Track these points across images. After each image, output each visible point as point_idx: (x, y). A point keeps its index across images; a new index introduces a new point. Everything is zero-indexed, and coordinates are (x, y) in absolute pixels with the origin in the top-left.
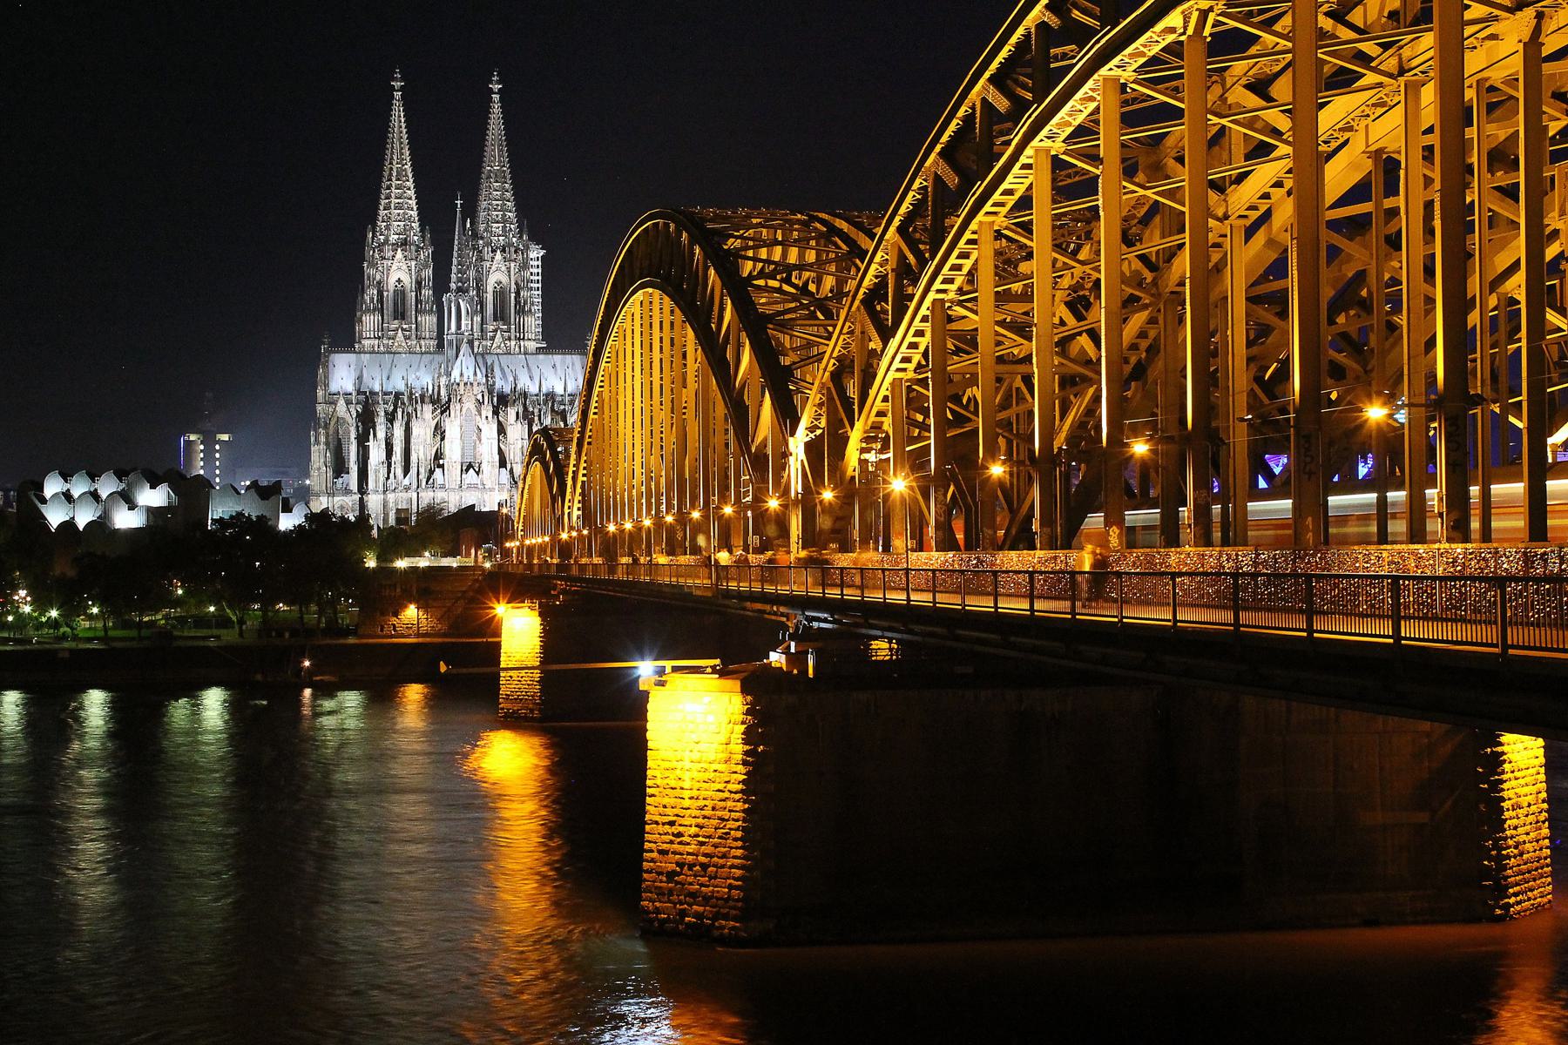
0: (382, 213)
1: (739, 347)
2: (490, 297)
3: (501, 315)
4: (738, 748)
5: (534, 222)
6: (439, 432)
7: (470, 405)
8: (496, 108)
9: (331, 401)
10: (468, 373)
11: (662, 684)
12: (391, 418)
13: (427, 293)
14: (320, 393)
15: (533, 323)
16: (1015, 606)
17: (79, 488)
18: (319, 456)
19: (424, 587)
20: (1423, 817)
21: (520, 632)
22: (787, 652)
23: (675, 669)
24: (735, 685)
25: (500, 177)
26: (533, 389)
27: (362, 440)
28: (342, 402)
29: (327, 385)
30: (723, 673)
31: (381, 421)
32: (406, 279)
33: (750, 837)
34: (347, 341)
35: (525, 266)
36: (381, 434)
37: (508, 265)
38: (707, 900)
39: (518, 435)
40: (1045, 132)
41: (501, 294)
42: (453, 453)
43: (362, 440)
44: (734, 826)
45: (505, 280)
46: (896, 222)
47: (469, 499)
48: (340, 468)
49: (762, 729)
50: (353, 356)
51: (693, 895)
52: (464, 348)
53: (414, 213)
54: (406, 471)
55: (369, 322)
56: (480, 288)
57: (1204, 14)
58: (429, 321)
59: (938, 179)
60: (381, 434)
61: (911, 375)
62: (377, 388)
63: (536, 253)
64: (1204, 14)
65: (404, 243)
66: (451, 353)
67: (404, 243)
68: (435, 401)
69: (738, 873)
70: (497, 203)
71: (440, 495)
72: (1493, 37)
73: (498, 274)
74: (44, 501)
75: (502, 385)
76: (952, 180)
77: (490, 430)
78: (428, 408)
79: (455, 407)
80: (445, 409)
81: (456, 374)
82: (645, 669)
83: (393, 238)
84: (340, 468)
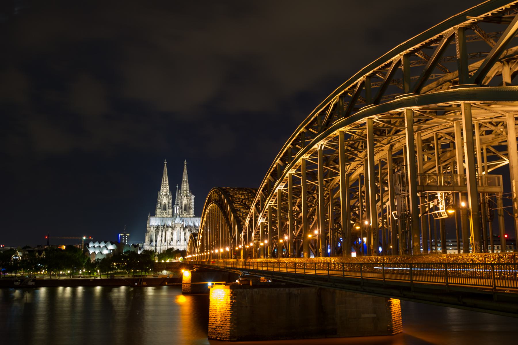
0: (162, 189)
1: (231, 215)
2: (183, 206)
3: (185, 210)
4: (229, 301)
5: (193, 190)
6: (172, 234)
7: (179, 228)
8: (185, 168)
11: (212, 287)
13: (170, 205)
14: (148, 225)
15: (192, 211)
16: (284, 270)
17: (96, 245)
18: (147, 239)
19: (168, 267)
20: (375, 315)
21: (186, 275)
22: (240, 280)
23: (216, 284)
24: (229, 287)
25: (186, 181)
26: (192, 225)
27: (156, 236)
28: (152, 228)
30: (226, 285)
31: (160, 231)
33: (231, 321)
34: (154, 214)
35: (191, 199)
36: (160, 234)
37: (187, 198)
38: (222, 334)
39: (188, 234)
40: (291, 170)
41: (186, 206)
42: (175, 238)
43: (156, 236)
44: (228, 318)
45: (186, 202)
46: (262, 189)
47: (178, 247)
48: (151, 241)
49: (234, 296)
50: (154, 218)
51: (219, 333)
52: (178, 216)
53: (168, 189)
54: (165, 242)
55: (158, 211)
56: (181, 204)
57: (322, 145)
58: (171, 211)
59: (269, 180)
60: (160, 234)
61: (264, 221)
64: (322, 145)
65: (166, 195)
66: (175, 217)
67: (166, 195)
68: (171, 227)
69: (229, 328)
70: (185, 187)
71: (172, 247)
72: (383, 150)
73: (185, 201)
74: (89, 248)
75: (185, 224)
76: (272, 180)
77: (183, 233)
78: (170, 229)
79: (175, 229)
81: (176, 222)
82: (210, 284)
83: (164, 194)
84: (151, 241)
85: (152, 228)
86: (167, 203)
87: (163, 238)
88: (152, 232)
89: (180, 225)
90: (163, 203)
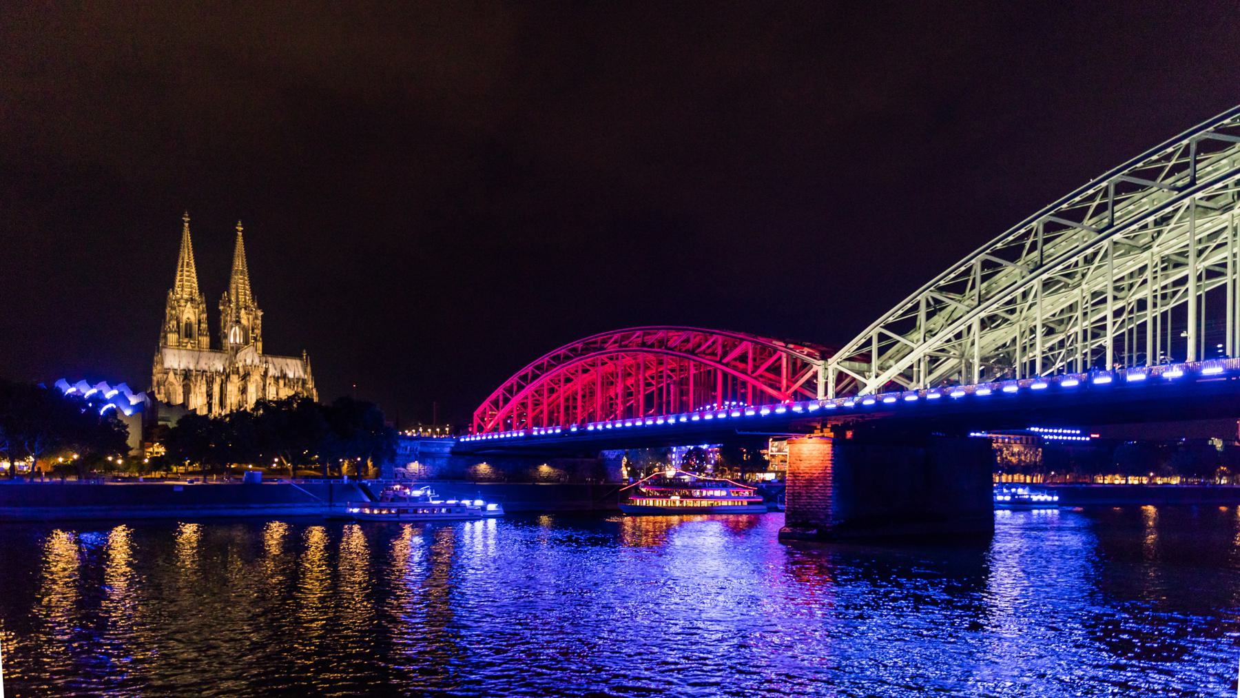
6: (244, 391)
9: (166, 372)
10: (257, 361)
12: (210, 383)
13: (204, 326)
14: (156, 369)
15: (260, 345)
28: (171, 374)
29: (163, 364)
32: (193, 319)
37: (244, 316)
55: (172, 338)
58: (205, 340)
60: (204, 389)
62: (192, 367)
63: (260, 313)
80: (245, 377)
83: (186, 296)
85: (171, 374)
86: (193, 319)
87: (216, 400)
88: (171, 384)
89: (262, 371)
90: (184, 318)
